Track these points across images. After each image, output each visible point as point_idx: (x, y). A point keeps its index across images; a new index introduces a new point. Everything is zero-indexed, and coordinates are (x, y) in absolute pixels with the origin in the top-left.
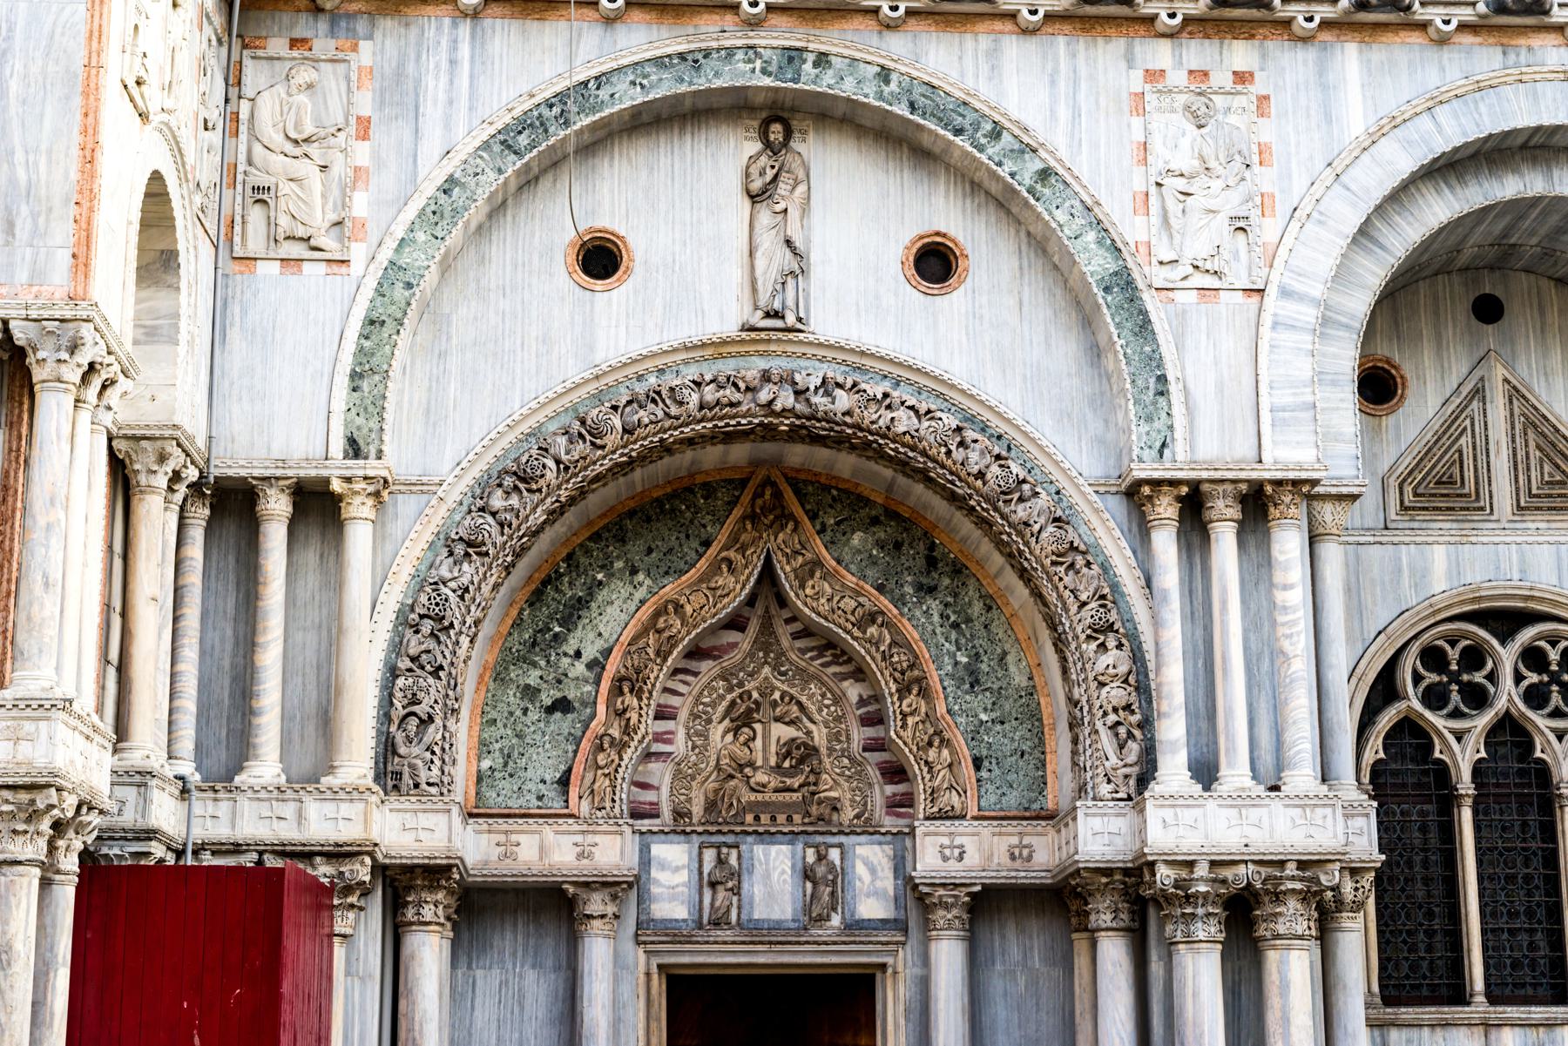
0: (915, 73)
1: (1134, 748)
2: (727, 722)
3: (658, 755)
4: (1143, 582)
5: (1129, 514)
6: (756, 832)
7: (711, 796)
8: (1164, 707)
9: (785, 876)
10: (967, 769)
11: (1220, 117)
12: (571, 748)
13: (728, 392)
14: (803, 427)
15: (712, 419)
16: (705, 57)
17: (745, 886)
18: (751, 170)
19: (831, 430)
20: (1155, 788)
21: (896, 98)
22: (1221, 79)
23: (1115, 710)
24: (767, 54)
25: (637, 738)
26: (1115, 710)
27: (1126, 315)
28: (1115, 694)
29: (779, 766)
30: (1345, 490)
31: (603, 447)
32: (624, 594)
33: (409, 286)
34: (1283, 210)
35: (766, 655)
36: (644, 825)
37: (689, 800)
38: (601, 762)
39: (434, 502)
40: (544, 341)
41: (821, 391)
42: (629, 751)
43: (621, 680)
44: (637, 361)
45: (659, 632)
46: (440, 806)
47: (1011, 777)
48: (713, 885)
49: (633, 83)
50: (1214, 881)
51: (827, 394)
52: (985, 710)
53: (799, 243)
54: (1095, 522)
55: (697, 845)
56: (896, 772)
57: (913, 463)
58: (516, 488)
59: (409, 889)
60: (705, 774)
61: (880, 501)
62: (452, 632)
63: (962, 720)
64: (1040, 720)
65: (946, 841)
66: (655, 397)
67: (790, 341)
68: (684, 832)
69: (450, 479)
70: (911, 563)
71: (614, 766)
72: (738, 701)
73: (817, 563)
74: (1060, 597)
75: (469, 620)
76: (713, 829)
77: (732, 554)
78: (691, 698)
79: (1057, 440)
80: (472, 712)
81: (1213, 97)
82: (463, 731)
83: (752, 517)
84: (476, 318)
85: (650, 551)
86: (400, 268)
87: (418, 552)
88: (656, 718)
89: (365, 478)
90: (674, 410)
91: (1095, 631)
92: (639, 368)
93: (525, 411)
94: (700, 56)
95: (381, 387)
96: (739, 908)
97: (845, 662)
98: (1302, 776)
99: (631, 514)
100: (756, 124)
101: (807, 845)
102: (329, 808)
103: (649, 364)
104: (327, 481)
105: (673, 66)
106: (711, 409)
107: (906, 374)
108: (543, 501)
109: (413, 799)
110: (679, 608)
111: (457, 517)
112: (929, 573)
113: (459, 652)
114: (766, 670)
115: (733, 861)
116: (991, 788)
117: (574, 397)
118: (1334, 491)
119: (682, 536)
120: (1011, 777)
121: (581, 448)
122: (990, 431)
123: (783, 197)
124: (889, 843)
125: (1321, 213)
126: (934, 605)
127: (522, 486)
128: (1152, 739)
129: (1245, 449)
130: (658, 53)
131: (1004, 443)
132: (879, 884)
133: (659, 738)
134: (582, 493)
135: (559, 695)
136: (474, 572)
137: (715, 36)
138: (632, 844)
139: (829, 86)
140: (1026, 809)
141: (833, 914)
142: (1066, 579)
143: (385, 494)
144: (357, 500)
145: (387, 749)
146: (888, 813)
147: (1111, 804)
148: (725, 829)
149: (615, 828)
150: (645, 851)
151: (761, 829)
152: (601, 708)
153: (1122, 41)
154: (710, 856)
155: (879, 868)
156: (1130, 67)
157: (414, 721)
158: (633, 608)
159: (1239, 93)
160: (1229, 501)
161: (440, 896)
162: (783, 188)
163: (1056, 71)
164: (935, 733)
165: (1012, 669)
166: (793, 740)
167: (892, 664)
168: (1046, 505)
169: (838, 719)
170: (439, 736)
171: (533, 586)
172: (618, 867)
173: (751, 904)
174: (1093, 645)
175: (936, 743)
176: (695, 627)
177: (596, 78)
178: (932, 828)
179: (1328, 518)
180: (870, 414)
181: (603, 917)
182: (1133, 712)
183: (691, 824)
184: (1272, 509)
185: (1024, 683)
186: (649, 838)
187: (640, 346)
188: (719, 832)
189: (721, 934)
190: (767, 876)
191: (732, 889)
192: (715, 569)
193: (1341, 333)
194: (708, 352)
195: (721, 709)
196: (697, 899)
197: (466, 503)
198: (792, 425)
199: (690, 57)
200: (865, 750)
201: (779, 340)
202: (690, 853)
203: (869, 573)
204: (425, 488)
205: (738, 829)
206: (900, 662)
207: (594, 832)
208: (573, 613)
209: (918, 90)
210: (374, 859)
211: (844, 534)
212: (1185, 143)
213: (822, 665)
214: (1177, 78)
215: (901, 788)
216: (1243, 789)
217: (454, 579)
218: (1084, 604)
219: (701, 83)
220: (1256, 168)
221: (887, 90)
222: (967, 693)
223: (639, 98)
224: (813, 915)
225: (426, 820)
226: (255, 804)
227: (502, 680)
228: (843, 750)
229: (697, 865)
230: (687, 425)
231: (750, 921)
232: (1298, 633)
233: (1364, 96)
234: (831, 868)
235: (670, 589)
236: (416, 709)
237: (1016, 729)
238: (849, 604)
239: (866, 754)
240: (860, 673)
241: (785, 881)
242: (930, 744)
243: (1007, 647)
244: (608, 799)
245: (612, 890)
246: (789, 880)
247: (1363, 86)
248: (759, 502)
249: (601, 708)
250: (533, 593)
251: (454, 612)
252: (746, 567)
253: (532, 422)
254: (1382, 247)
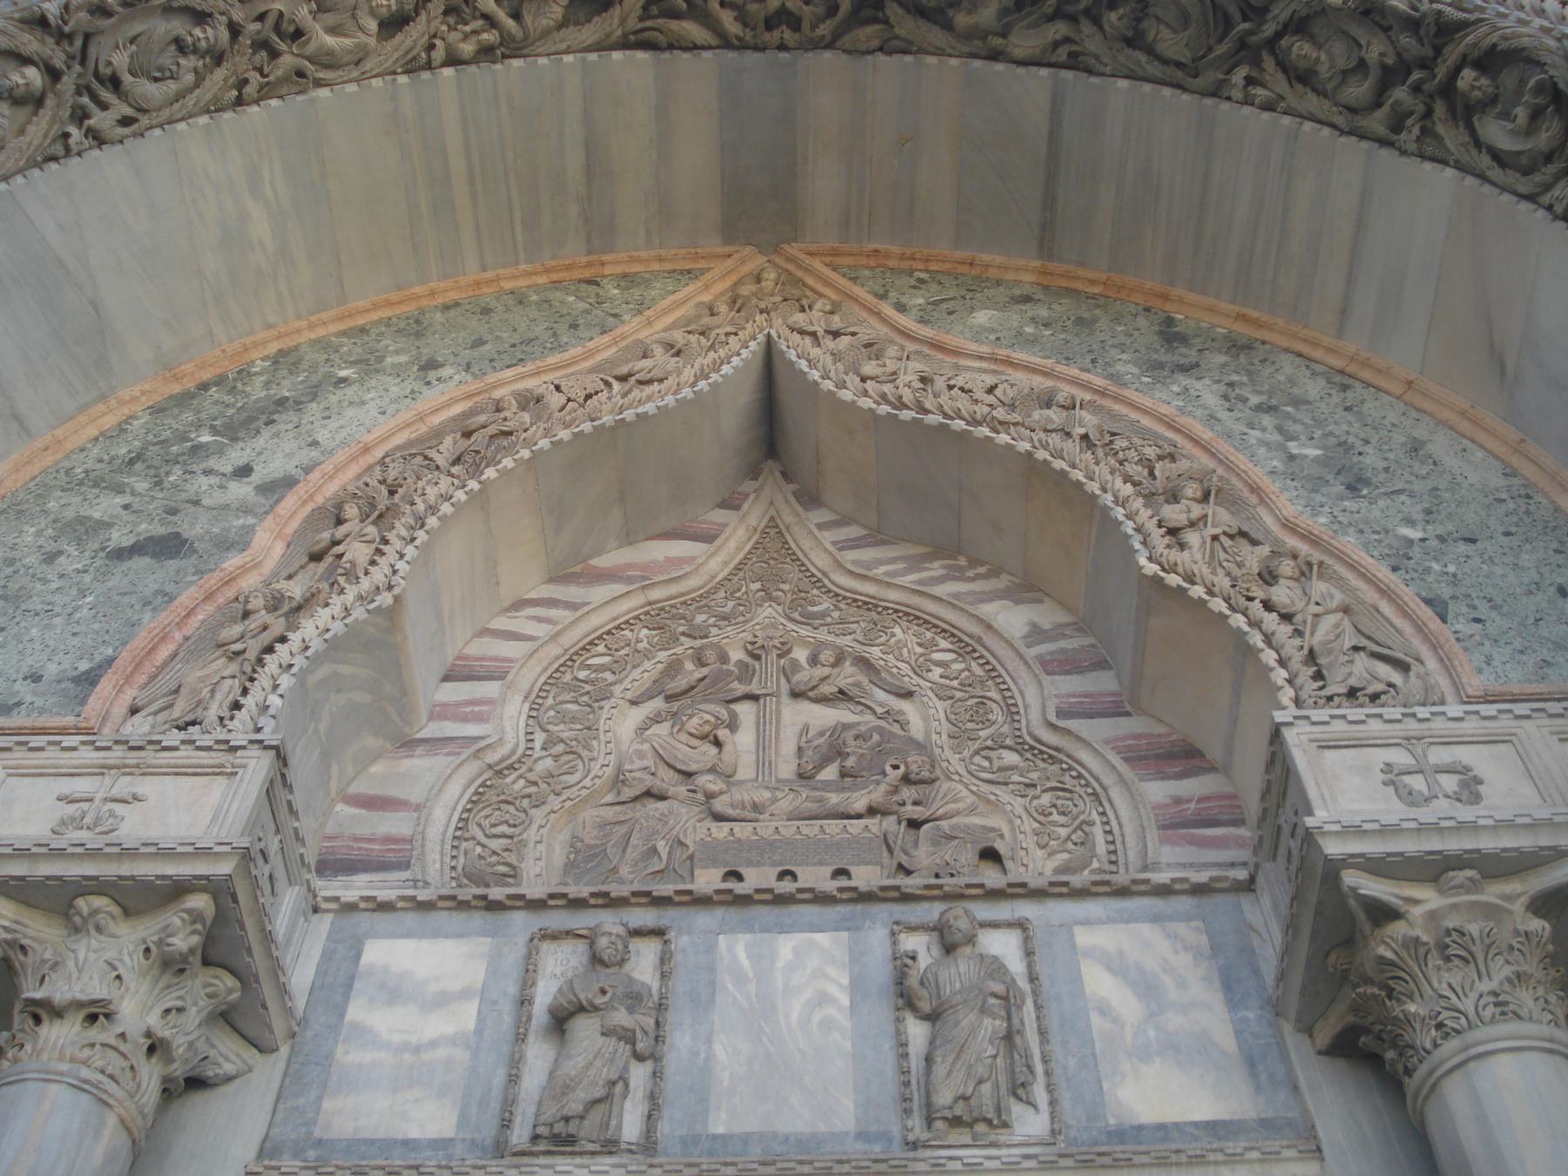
9: (829, 1011)
17: (681, 1042)
42: (323, 615)
52: (1409, 522)
55: (522, 940)
65: (1400, 757)
70: (1122, 339)
71: (266, 638)
72: (689, 666)
78: (554, 650)
124: (1188, 918)
132: (1174, 1021)
133: (442, 712)
141: (1017, 1109)
146: (1163, 841)
155: (1167, 980)
171: (177, 389)
178: (1339, 727)
186: (364, 920)
191: (627, 1036)
196: (500, 1076)
211: (951, 313)
227: (18, 512)
229: (512, 989)
234: (996, 968)
241: (828, 1024)
246: (844, 1021)
250: (171, 397)
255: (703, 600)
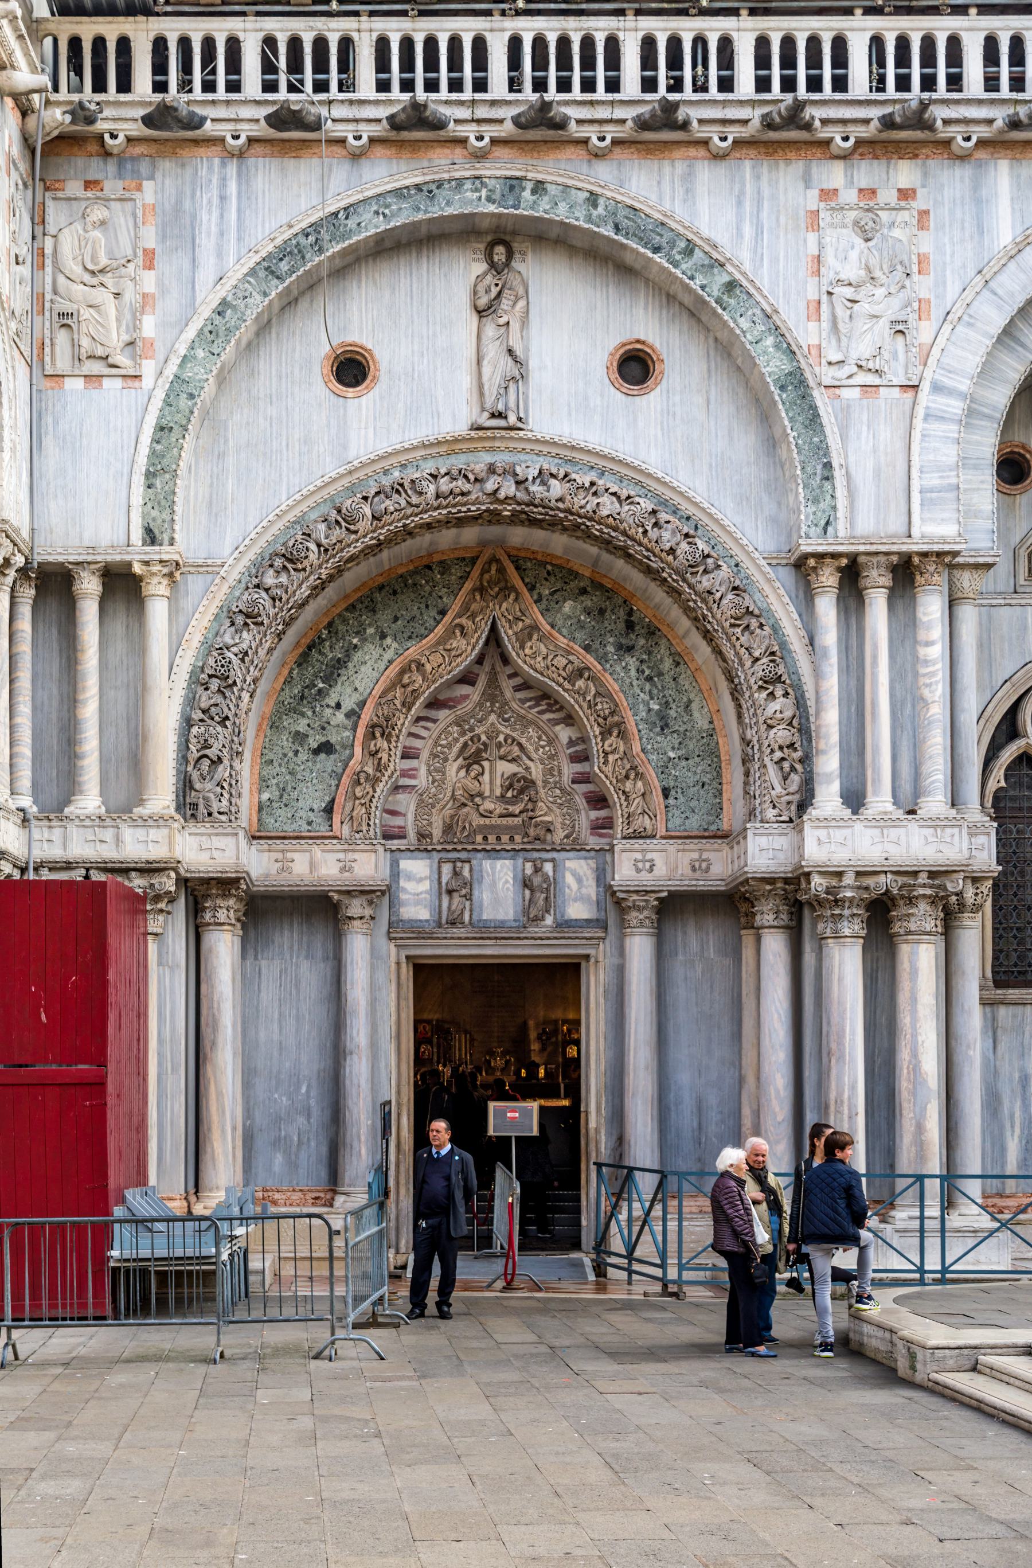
0: (619, 198)
1: (795, 779)
2: (460, 760)
3: (405, 787)
4: (807, 641)
5: (797, 582)
6: (484, 850)
7: (448, 821)
8: (822, 745)
10: (657, 797)
11: (885, 231)
12: (334, 783)
13: (460, 483)
14: (523, 512)
15: (446, 507)
16: (438, 187)
17: (476, 893)
18: (478, 288)
19: (547, 514)
20: (813, 812)
21: (602, 221)
22: (888, 196)
23: (781, 748)
24: (490, 183)
25: (387, 774)
26: (781, 748)
27: (799, 410)
28: (781, 735)
29: (503, 796)
30: (981, 560)
31: (356, 532)
32: (376, 654)
33: (191, 396)
34: (937, 313)
35: (493, 705)
36: (394, 844)
37: (430, 824)
38: (359, 794)
39: (217, 581)
40: (305, 442)
41: (538, 481)
42: (381, 785)
43: (374, 726)
44: (383, 457)
45: (404, 686)
46: (229, 830)
47: (694, 804)
48: (450, 892)
49: (377, 213)
50: (859, 888)
52: (673, 748)
53: (519, 352)
54: (768, 590)
56: (598, 801)
57: (615, 542)
58: (284, 567)
59: (207, 896)
60: (443, 803)
61: (587, 574)
62: (235, 689)
63: (654, 757)
64: (718, 756)
66: (398, 488)
67: (512, 438)
68: (426, 850)
69: (230, 561)
70: (613, 627)
73: (535, 627)
74: (737, 654)
75: (249, 679)
76: (450, 847)
77: (464, 621)
79: (737, 520)
80: (253, 755)
81: (879, 213)
82: (246, 770)
83: (481, 589)
84: (248, 423)
85: (396, 619)
86: (184, 381)
87: (205, 623)
88: (402, 758)
89: (161, 562)
90: (415, 500)
91: (766, 682)
92: (385, 464)
93: (290, 502)
94: (433, 187)
95: (170, 484)
96: (471, 910)
97: (558, 710)
98: (935, 803)
99: (381, 588)
100: (482, 246)
101: (526, 860)
102: (140, 833)
103: (394, 460)
104: (129, 565)
105: (410, 196)
106: (445, 498)
107: (610, 465)
108: (307, 578)
109: (208, 825)
110: (420, 666)
111: (237, 593)
112: (627, 634)
113: (241, 705)
114: (493, 717)
115: (466, 873)
116: (677, 813)
117: (331, 490)
118: (972, 560)
119: (423, 606)
120: (694, 804)
121: (338, 533)
122: (680, 513)
123: (505, 312)
125: (971, 316)
126: (632, 662)
127: (289, 566)
128: (811, 772)
130: (398, 185)
131: (692, 523)
132: (584, 891)
133: (404, 774)
134: (340, 571)
135: (323, 739)
136: (251, 638)
137: (446, 168)
138: (384, 859)
139: (545, 212)
140: (705, 830)
142: (742, 639)
143: (177, 574)
144: (155, 580)
145: (185, 785)
147: (776, 825)
148: (459, 847)
149: (370, 847)
150: (395, 864)
151: (488, 848)
152: (358, 750)
153: (801, 163)
154: (447, 869)
156: (807, 187)
157: (206, 762)
158: (383, 667)
159: (902, 209)
160: (882, 571)
161: (231, 902)
162: (505, 304)
163: (742, 192)
164: (632, 768)
165: (696, 714)
166: (515, 775)
167: (596, 711)
168: (726, 576)
169: (552, 757)
170: (227, 774)
172: (373, 878)
173: (481, 907)
174: (764, 694)
175: (632, 776)
176: (433, 682)
177: (345, 209)
179: (966, 584)
181: (361, 918)
182: (795, 750)
183: (431, 844)
184: (918, 577)
185: (706, 726)
186: (398, 854)
187: (385, 445)
188: (455, 850)
189: (457, 932)
190: (494, 884)
192: (450, 633)
193: (983, 423)
194: (442, 449)
195: (456, 749)
197: (243, 581)
198: (514, 510)
199: (425, 188)
200: (573, 782)
201: (502, 437)
202: (431, 867)
203: (577, 635)
204: (210, 569)
205: (470, 847)
206: (603, 709)
207: (353, 851)
208: (334, 671)
209: (622, 213)
210: (177, 873)
213: (539, 713)
214: (849, 196)
215: (603, 813)
216: (885, 813)
217: (236, 644)
218: (757, 660)
219: (435, 212)
220: (915, 277)
221: (595, 213)
222: (658, 734)
223: (381, 225)
224: (530, 917)
225: (218, 842)
226: (82, 830)
228: (556, 783)
230: (426, 512)
231: (480, 921)
232: (937, 683)
233: (1013, 209)
235: (413, 651)
236: (207, 752)
237: (698, 764)
238: (561, 661)
239: (575, 786)
240: (569, 720)
242: (627, 777)
243: (692, 696)
244: (364, 824)
245: (369, 897)
247: (1012, 199)
248: (486, 576)
249: (358, 750)
251: (237, 672)
252: (476, 631)
253: (297, 512)
254: (1023, 345)
255: (472, 714)
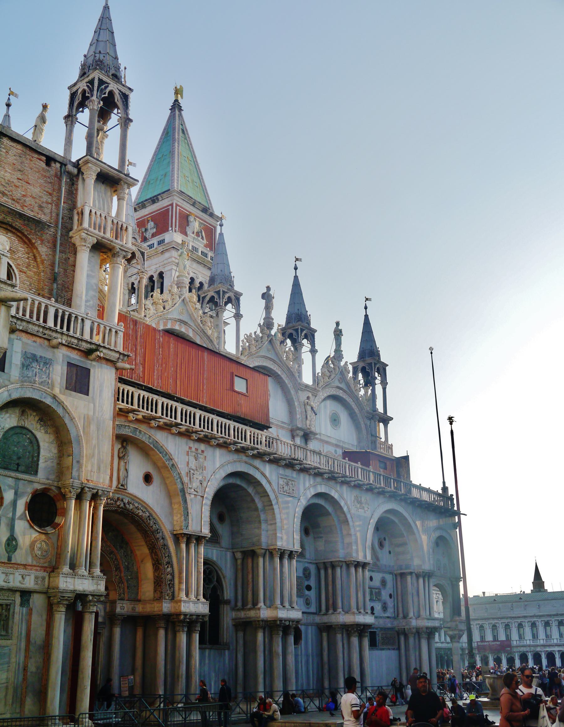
22: (200, 451)
51: (129, 505)
129: (199, 529)
180: (135, 510)
212: (194, 463)
